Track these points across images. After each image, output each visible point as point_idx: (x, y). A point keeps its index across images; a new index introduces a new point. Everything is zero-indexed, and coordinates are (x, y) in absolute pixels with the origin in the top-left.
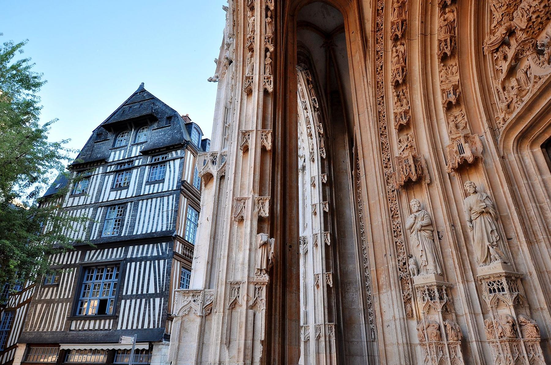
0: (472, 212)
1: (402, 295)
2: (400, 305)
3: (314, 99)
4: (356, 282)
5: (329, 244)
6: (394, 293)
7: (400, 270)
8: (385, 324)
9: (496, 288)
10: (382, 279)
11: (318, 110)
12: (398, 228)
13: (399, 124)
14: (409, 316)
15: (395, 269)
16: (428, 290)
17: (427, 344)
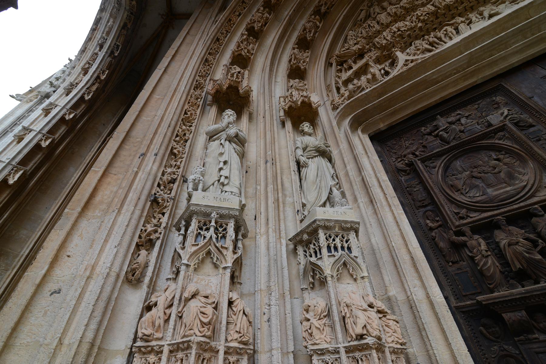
0: (308, 149)
1: (140, 227)
2: (125, 244)
3: (118, 46)
4: (17, 256)
5: (11, 182)
6: (123, 219)
7: (159, 185)
8: (51, 286)
9: (339, 245)
10: (107, 192)
11: (115, 57)
12: (185, 134)
13: (239, 53)
14: (133, 278)
15: (151, 178)
16: (216, 222)
17: (166, 350)
